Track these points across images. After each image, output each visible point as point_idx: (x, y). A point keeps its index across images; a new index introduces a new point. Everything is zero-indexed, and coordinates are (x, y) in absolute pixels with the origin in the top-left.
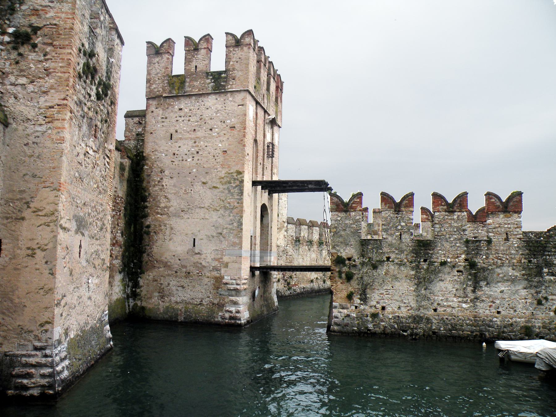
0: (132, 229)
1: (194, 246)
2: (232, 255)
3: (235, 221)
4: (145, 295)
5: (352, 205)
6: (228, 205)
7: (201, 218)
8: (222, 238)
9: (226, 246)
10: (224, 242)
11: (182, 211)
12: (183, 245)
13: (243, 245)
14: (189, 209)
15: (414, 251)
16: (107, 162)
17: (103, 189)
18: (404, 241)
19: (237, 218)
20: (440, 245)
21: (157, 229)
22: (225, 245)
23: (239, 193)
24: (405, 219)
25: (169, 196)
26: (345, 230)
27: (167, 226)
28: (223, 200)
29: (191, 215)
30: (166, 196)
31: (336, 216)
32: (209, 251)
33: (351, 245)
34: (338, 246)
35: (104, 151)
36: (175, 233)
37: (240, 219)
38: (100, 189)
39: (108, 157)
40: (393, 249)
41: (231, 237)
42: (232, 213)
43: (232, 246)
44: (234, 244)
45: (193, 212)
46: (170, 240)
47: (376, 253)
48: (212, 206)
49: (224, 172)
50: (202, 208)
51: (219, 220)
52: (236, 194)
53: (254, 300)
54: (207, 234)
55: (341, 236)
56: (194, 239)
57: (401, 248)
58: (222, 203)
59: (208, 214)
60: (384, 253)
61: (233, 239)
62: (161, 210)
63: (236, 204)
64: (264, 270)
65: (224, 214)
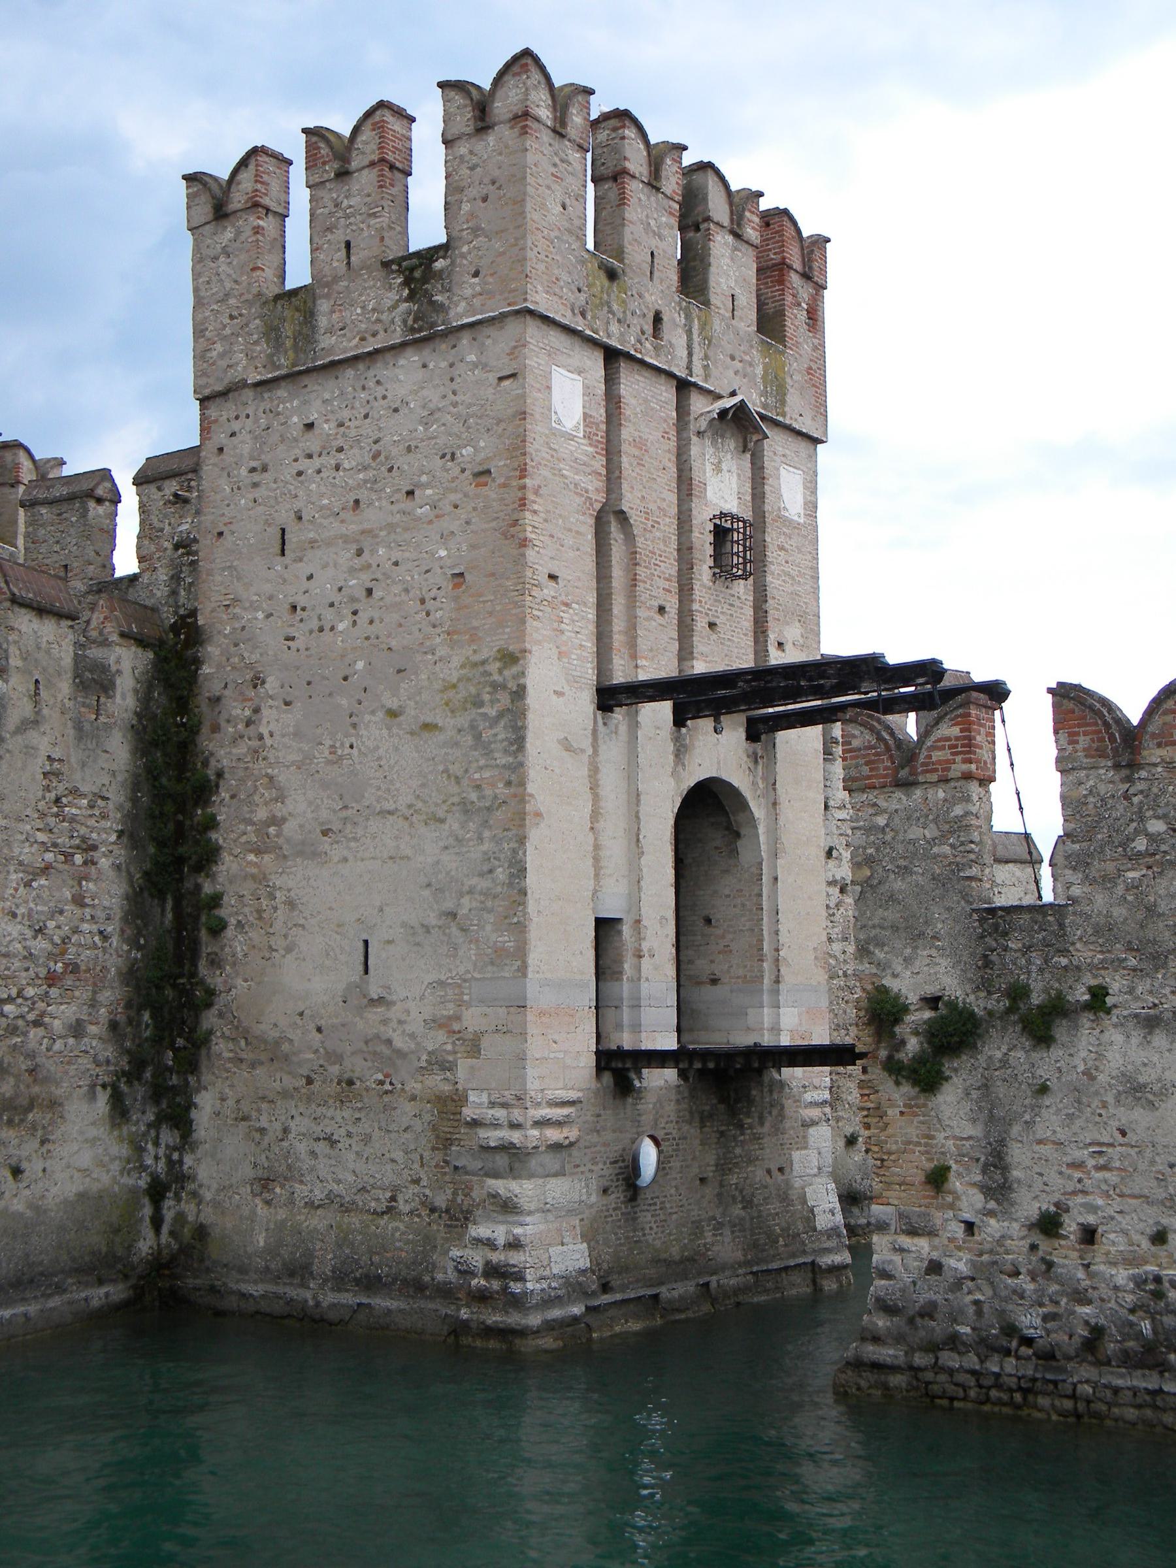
0: (170, 915)
1: (366, 972)
5: (930, 757)
6: (473, 796)
11: (325, 833)
13: (532, 959)
14: (345, 820)
23: (512, 744)
24: (1163, 801)
25: (282, 778)
27: (278, 894)
28: (457, 777)
29: (353, 844)
30: (271, 778)
31: (871, 811)
33: (934, 938)
36: (302, 921)
37: (515, 851)
40: (1119, 951)
41: (489, 928)
42: (490, 827)
43: (492, 964)
44: (499, 956)
45: (360, 832)
46: (289, 950)
48: (420, 805)
50: (390, 813)
51: (445, 858)
52: (499, 746)
55: (892, 898)
56: (366, 942)
57: (1155, 942)
58: (455, 789)
59: (407, 838)
60: (1078, 968)
61: (494, 937)
62: (257, 832)
63: (501, 790)
65: (461, 832)
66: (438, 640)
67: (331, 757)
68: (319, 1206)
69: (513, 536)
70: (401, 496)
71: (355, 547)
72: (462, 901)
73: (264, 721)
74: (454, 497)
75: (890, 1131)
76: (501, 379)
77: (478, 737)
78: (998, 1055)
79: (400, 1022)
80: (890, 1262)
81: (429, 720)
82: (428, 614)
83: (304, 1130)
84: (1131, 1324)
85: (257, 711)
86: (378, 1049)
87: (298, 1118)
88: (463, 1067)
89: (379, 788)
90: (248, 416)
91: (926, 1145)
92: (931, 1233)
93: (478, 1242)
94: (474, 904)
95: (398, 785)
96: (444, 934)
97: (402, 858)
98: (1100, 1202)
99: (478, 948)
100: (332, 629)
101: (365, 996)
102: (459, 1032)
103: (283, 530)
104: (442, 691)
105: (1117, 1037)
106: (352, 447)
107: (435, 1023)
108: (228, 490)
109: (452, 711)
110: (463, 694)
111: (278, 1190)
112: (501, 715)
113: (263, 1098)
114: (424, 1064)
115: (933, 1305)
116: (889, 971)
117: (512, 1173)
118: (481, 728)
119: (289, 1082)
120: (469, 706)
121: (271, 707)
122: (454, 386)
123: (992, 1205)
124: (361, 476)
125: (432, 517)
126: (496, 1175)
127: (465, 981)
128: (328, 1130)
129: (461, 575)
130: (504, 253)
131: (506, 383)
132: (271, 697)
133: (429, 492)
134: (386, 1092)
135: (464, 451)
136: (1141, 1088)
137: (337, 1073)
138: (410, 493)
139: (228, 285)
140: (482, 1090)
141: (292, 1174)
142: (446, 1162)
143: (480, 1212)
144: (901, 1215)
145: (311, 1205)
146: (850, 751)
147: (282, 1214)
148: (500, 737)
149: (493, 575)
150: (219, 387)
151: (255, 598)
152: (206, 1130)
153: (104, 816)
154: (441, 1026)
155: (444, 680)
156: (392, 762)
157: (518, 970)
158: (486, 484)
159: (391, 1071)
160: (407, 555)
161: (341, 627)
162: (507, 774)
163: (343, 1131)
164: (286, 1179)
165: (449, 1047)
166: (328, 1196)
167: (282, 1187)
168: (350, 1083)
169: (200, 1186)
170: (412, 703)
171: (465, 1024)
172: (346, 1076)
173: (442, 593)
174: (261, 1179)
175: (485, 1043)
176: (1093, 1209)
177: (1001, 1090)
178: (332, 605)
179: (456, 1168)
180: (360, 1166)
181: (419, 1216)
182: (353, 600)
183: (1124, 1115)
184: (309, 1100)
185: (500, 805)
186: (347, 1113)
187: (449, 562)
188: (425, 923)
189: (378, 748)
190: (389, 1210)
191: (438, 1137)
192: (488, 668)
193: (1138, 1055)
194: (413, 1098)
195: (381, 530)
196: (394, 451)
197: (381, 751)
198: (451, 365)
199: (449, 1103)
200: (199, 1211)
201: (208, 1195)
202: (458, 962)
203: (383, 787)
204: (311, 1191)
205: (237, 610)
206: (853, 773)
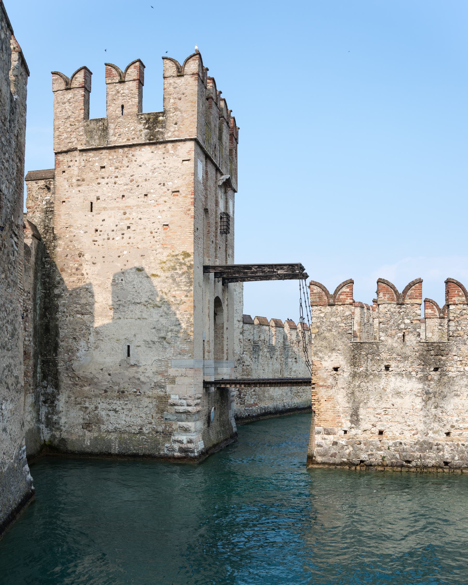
1: (129, 355)
2: (180, 367)
3: (183, 321)
4: (65, 423)
5: (339, 297)
6: (172, 299)
7: (136, 317)
8: (166, 344)
9: (171, 355)
10: (169, 349)
12: (114, 354)
14: (119, 305)
15: (422, 358)
16: (15, 242)
17: (12, 281)
18: (408, 343)
19: (185, 316)
20: (455, 349)
21: (78, 334)
22: (170, 352)
23: (188, 283)
26: (330, 330)
27: (91, 329)
28: (165, 293)
29: (123, 313)
32: (150, 362)
34: (321, 352)
35: (11, 226)
36: (102, 338)
38: (9, 279)
39: (16, 235)
40: (394, 355)
41: (178, 343)
42: (179, 310)
43: (180, 354)
45: (126, 309)
46: (96, 348)
47: (371, 360)
49: (166, 253)
50: (138, 303)
51: (161, 319)
53: (209, 426)
54: (145, 339)
55: (325, 338)
56: (129, 346)
59: (146, 312)
61: (181, 346)
64: (223, 386)
65: (167, 311)
66: (158, 246)
67: (113, 283)
68: (111, 432)
69: (188, 214)
70: (143, 196)
71: (122, 212)
72: (168, 334)
73: (84, 269)
75: (322, 405)
76: (183, 161)
77: (174, 280)
78: (357, 384)
79: (143, 372)
80: (322, 442)
81: (154, 273)
82: (154, 237)
83: (104, 407)
84: (394, 455)
85: (81, 265)
86: (134, 381)
87: (101, 404)
88: (168, 388)
89: (134, 295)
90: (76, 161)
91: (333, 409)
92: (334, 434)
93: (175, 441)
94: (173, 335)
95: (142, 294)
96: (161, 344)
97: (143, 319)
98: (385, 424)
99: (174, 349)
100: (113, 239)
101: (128, 364)
102: (167, 376)
103: (92, 203)
104: (159, 264)
105: (393, 379)
106: (121, 177)
107: (157, 373)
108: (67, 186)
109: (164, 271)
110: (169, 265)
111: (94, 427)
112: (183, 273)
113: (86, 397)
114: (153, 386)
115: (336, 454)
116: (323, 360)
117: (187, 420)
118: (175, 277)
119: (97, 392)
120: (170, 269)
121: (87, 264)
122: (165, 160)
123: (353, 425)
124: (125, 187)
125: (155, 204)
126: (182, 421)
127: (169, 359)
128: (114, 407)
129: (167, 225)
131: (184, 162)
132: (87, 261)
133: (154, 196)
134: (138, 395)
135: (169, 183)
136: (400, 393)
137: (118, 389)
138: (146, 195)
139: (70, 113)
140: (176, 395)
141: (99, 421)
142: (162, 417)
143: (176, 432)
144: (325, 429)
145: (108, 432)
146: (313, 293)
147: (96, 435)
148: (183, 281)
149: (181, 226)
150: (65, 149)
151: (80, 226)
152: (62, 407)
153: (29, 300)
154: (159, 374)
156: (139, 286)
157: (190, 357)
158: (178, 196)
159: (139, 388)
160: (145, 216)
161: (117, 238)
162: (185, 293)
163: (120, 408)
164: (97, 423)
165: (163, 381)
166: (115, 429)
167: (95, 426)
168: (123, 392)
169: (61, 426)
170: (148, 267)
171: (169, 373)
172: (122, 390)
173: (159, 230)
174: (86, 424)
175: (177, 379)
176: (383, 425)
177: (357, 394)
178: (113, 231)
179: (166, 419)
180: (128, 419)
181: (152, 434)
182: (122, 229)
183: (394, 401)
184: (106, 398)
185: (183, 303)
186: (121, 402)
187: (162, 220)
188: (153, 340)
189: (133, 281)
190: (139, 433)
191: (159, 409)
192: (178, 257)
193: (398, 384)
194: (149, 397)
195: (134, 206)
196: (140, 180)
197: (134, 283)
199: (163, 398)
200: (61, 434)
201: (64, 429)
202: (166, 354)
203: (135, 294)
204: (108, 427)
205: (72, 229)
206: (315, 300)
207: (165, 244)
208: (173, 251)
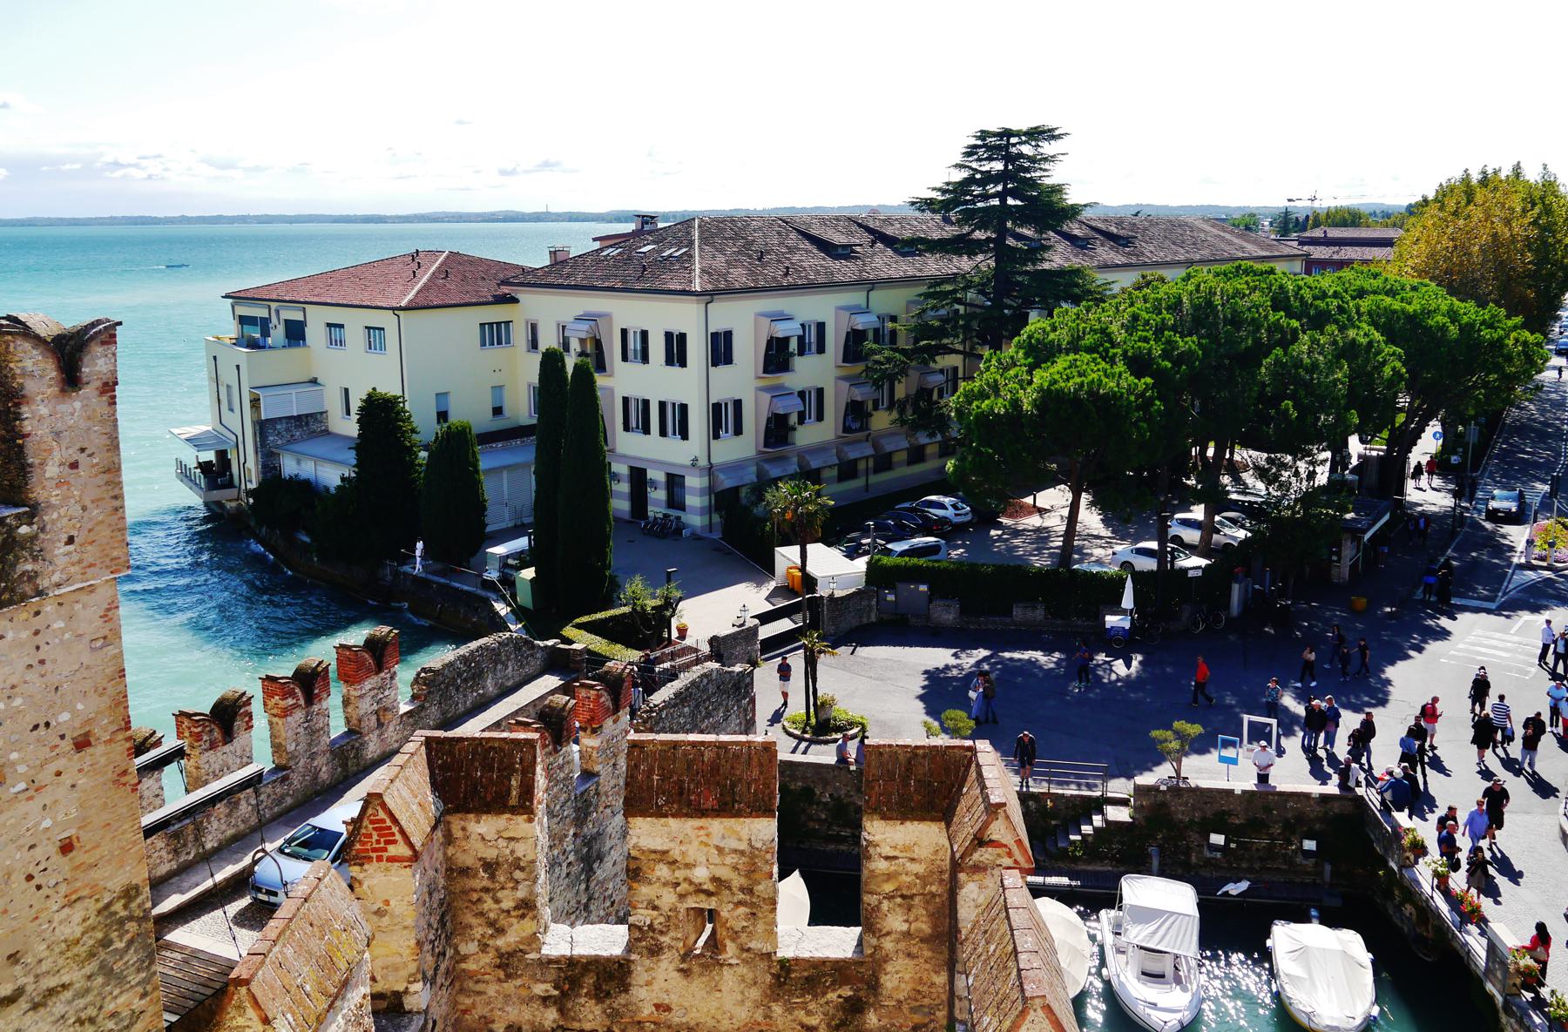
69: (124, 785)
74: (53, 768)
82: (39, 887)
110: (91, 942)
130: (102, 522)
148: (131, 962)
155: (66, 941)
185: (138, 1017)
192: (113, 909)
198: (37, 633)
207: (75, 891)
208: (97, 900)
